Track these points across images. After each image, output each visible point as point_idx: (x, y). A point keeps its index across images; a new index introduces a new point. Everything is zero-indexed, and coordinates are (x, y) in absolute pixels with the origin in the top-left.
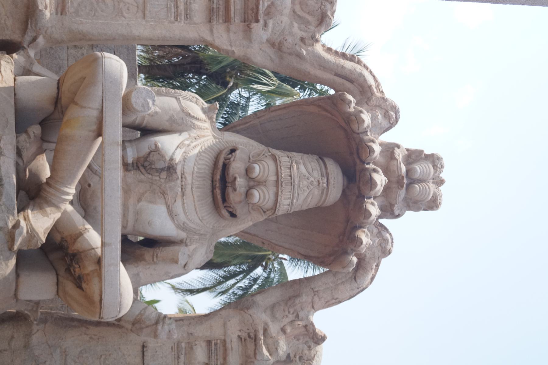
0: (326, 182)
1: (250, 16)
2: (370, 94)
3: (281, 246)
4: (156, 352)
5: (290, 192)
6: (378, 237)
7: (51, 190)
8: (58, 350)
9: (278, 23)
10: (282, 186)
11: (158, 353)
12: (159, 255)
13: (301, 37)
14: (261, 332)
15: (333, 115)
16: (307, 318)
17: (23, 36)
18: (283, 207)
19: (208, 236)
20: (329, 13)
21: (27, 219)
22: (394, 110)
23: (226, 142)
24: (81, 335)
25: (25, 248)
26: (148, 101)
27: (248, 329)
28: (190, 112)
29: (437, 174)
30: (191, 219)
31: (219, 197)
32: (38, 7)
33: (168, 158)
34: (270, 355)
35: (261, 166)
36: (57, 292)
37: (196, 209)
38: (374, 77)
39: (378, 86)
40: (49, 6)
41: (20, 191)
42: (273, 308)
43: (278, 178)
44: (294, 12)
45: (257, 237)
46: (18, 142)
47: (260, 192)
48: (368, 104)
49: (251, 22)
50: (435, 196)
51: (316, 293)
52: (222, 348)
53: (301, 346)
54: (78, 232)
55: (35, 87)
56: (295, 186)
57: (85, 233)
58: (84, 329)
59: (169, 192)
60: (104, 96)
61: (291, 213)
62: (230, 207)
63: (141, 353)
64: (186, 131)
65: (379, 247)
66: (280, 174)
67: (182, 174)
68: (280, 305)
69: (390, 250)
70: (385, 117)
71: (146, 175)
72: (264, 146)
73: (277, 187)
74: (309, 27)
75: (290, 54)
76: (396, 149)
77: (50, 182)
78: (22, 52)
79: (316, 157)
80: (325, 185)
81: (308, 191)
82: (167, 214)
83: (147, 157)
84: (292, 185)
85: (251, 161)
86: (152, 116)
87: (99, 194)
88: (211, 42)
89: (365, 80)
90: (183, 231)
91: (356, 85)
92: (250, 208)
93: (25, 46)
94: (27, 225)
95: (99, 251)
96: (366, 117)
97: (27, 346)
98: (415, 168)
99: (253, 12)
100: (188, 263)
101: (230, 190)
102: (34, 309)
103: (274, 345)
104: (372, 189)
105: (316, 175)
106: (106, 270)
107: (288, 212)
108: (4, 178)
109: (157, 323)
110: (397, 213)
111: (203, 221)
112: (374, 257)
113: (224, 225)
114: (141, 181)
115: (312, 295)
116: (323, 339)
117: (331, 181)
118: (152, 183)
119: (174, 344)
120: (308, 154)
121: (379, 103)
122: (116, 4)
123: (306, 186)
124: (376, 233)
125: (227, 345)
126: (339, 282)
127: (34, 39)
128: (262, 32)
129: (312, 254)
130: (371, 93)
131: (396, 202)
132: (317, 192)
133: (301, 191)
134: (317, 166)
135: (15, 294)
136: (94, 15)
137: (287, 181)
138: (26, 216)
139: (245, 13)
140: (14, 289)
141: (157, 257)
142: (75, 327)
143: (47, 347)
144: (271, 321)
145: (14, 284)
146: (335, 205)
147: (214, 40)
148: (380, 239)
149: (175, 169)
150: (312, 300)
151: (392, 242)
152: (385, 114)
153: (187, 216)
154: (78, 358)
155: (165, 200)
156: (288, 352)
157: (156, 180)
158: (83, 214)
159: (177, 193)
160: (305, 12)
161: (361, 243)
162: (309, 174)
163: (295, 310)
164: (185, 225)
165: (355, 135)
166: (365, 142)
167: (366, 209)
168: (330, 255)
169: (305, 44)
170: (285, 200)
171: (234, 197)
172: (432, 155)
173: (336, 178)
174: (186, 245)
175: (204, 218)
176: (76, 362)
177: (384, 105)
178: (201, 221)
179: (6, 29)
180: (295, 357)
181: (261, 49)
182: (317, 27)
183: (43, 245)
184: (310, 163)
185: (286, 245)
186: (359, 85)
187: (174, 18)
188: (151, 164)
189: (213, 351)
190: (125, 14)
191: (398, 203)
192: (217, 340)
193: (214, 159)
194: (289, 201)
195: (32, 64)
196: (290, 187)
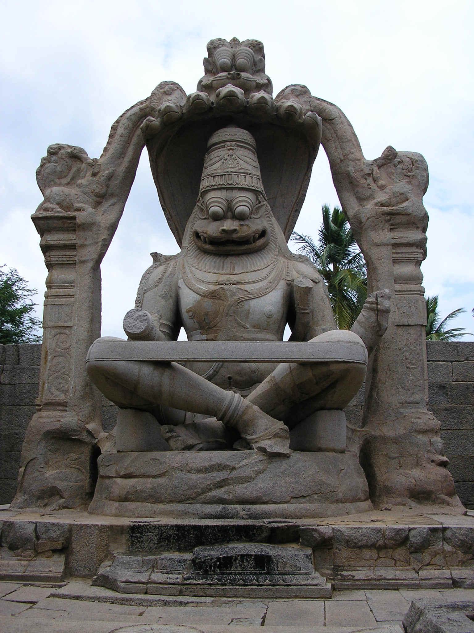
2: (148, 110)
3: (299, 193)
8: (402, 410)
9: (78, 198)
10: (232, 184)
12: (303, 307)
14: (385, 208)
17: (86, 443)
18: (254, 183)
19: (286, 261)
20: (69, 150)
21: (257, 440)
23: (190, 244)
25: (288, 442)
26: (137, 317)
28: (157, 279)
30: (266, 276)
32: (58, 429)
34: (408, 200)
36: (337, 409)
37: (255, 271)
38: (132, 107)
39: (141, 103)
40: (57, 419)
41: (234, 447)
42: (361, 200)
43: (224, 188)
44: (68, 184)
45: (290, 216)
47: (237, 205)
49: (75, 224)
53: (399, 171)
58: (380, 385)
60: (126, 359)
61: (260, 176)
62: (254, 236)
64: (177, 283)
65: (299, 97)
66: (220, 186)
68: (357, 192)
69: (303, 87)
75: (108, 186)
77: (220, 416)
78: (101, 446)
80: (233, 143)
81: (238, 160)
88: (94, 262)
89: (134, 114)
91: (140, 122)
93: (96, 441)
94: (263, 440)
95: (293, 365)
97: (396, 441)
98: (220, 64)
101: (235, 236)
102: (358, 434)
103: (398, 196)
104: (236, 95)
107: (259, 179)
108: (212, 463)
111: (269, 264)
112: (310, 102)
115: (348, 160)
117: (229, 138)
119: (396, 295)
121: (156, 100)
122: (57, 353)
127: (89, 432)
128: (84, 213)
131: (254, 81)
132: (241, 152)
134: (214, 152)
137: (227, 179)
138: (253, 441)
139: (68, 231)
142: (378, 393)
143: (397, 421)
144: (374, 198)
145: (327, 453)
147: (93, 259)
149: (213, 292)
150: (353, 161)
152: (167, 94)
154: (409, 390)
159: (238, 288)
160: (68, 173)
161: (292, 106)
166: (190, 106)
167: (257, 103)
169: (98, 172)
170: (247, 181)
172: (209, 49)
173: (227, 133)
175: (266, 263)
176: (412, 394)
179: (80, 460)
181: (103, 215)
182: (82, 161)
183: (285, 424)
186: (139, 120)
187: (72, 298)
189: (404, 256)
192: (393, 253)
194: (247, 177)
196: (233, 175)
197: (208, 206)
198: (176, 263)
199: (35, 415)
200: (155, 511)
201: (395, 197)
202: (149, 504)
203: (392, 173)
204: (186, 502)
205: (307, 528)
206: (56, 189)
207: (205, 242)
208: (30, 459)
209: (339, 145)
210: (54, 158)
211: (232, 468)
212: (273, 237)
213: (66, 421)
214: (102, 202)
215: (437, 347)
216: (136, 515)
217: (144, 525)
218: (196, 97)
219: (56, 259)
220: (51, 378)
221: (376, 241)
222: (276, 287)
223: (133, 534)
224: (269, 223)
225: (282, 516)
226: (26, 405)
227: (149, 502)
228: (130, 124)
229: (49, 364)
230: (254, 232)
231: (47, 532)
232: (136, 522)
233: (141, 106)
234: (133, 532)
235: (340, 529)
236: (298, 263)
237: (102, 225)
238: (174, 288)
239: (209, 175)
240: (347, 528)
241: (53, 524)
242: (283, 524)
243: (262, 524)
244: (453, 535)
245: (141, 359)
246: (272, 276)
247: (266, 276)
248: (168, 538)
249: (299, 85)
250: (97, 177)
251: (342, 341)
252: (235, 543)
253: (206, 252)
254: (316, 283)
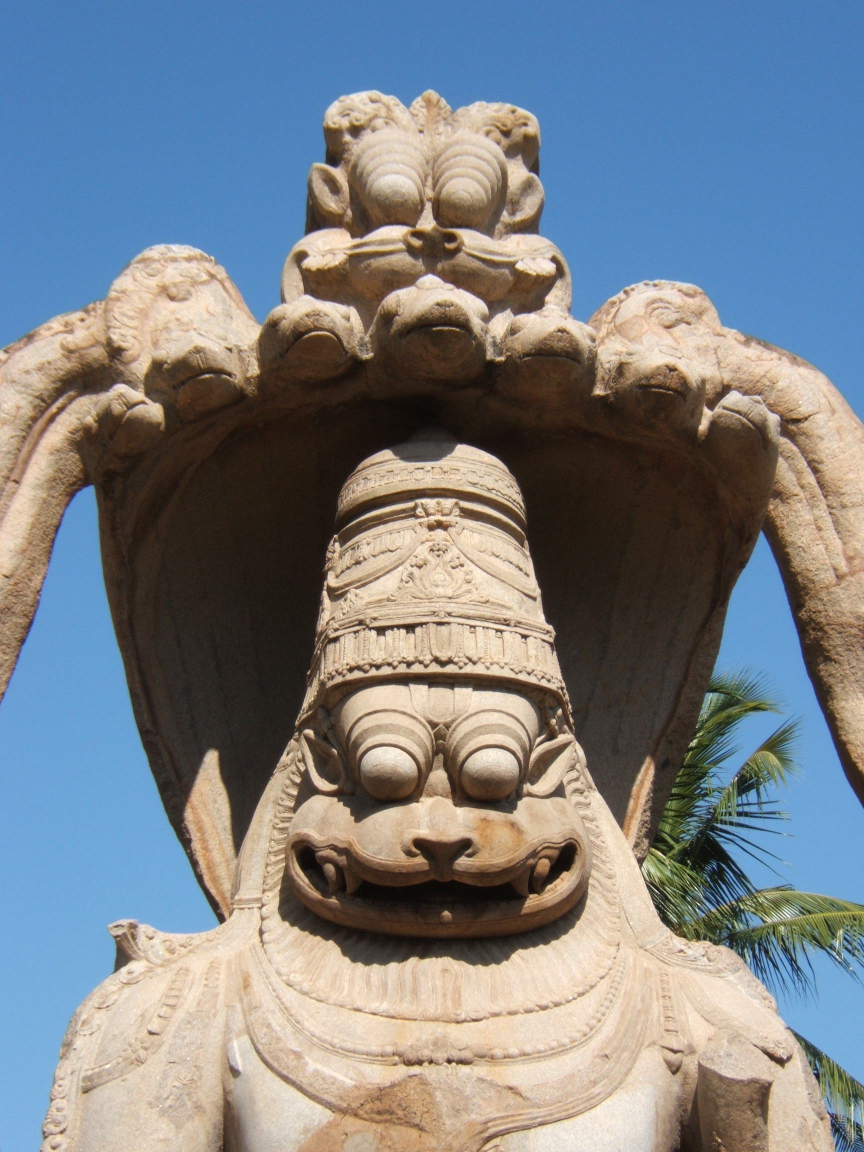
0: (436, 500)
2: (98, 353)
3: (678, 695)
10: (450, 661)
18: (533, 660)
22: (156, 266)
30: (586, 1029)
37: (544, 1008)
48: (134, 360)
50: (485, 125)
56: (449, 610)
59: (473, 1116)
61: (554, 633)
65: (675, 330)
66: (402, 669)
70: (184, 299)
72: (292, 742)
76: (308, 263)
79: (335, 547)
80: (448, 503)
81: (469, 566)
84: (449, 623)
89: (40, 369)
90: (634, 1059)
100: (761, 1044)
111: (592, 979)
113: (602, 901)
123: (450, 575)
124: (626, 342)
130: (93, 346)
133: (469, 591)
148: (646, 327)
149: (381, 1093)
152: (172, 298)
153: (574, 1045)
155: (507, 1132)
159: (482, 1080)
162: (403, 563)
164: (607, 1052)
170: (507, 651)
177: (140, 298)
178: (592, 987)
184: (358, 563)
186: (59, 392)
191: (512, 259)
197: (357, 745)
207: (340, 888)
209: (829, 519)
212: (599, 870)
218: (309, 322)
222: (626, 1074)
224: (582, 812)
228: (23, 403)
230: (534, 854)
233: (70, 338)
236: (699, 977)
239: (361, 623)
246: (608, 1028)
247: (586, 1029)
254: (781, 1062)
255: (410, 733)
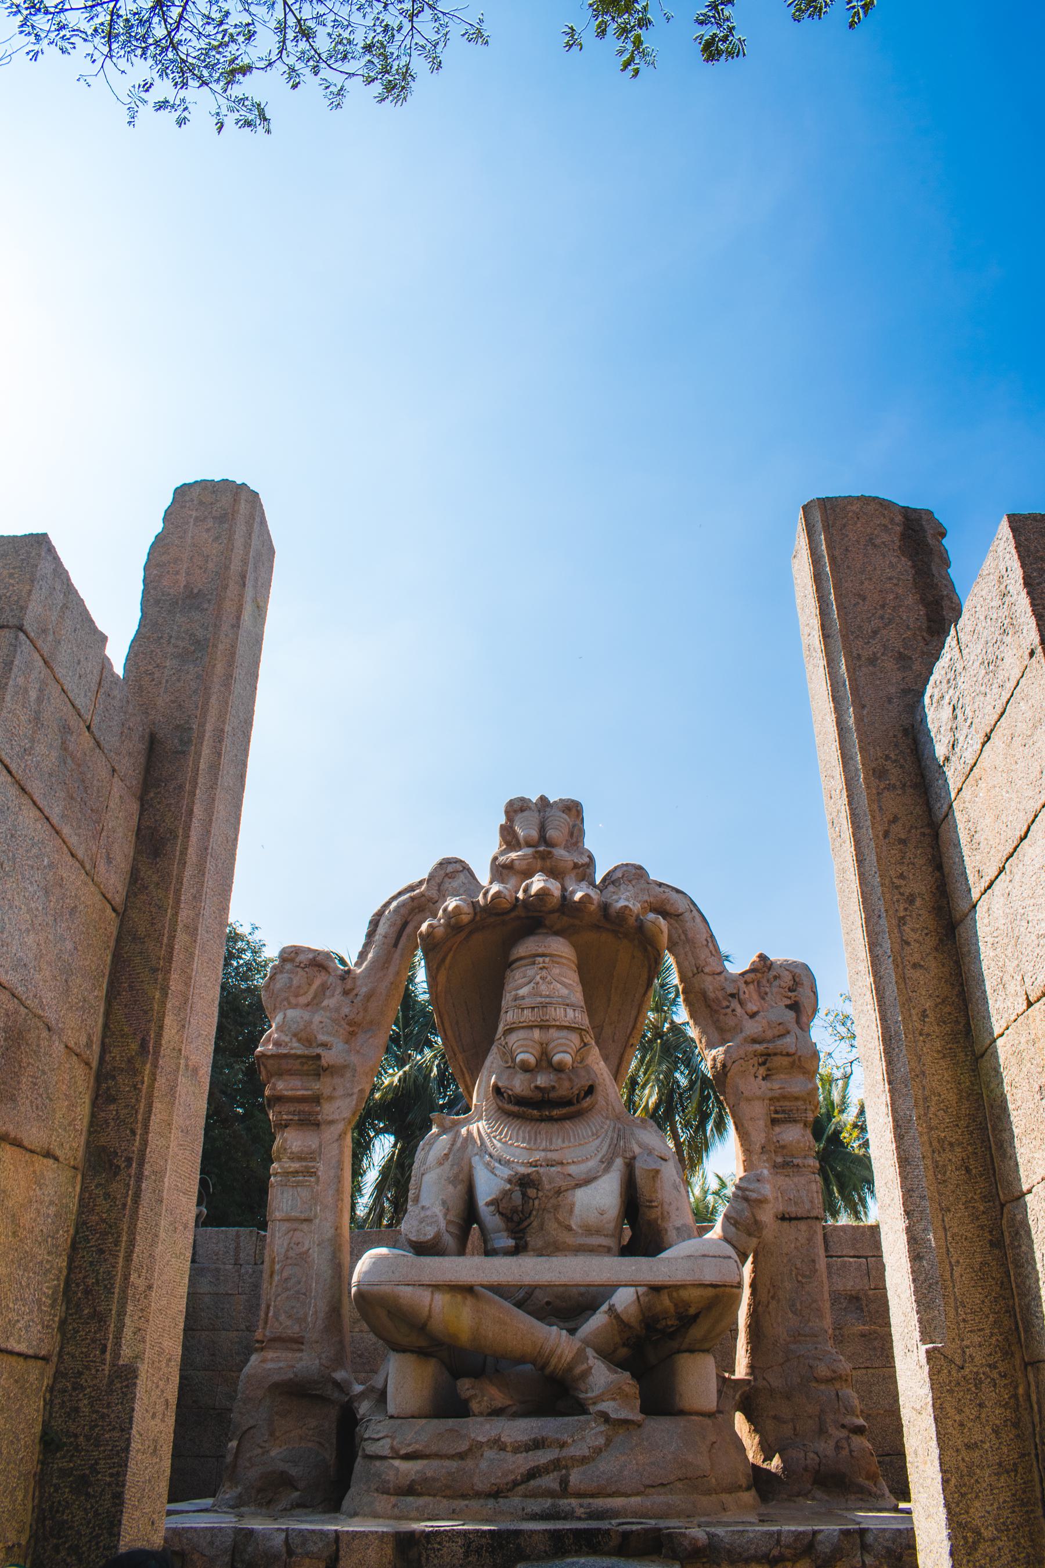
1: (311, 1068)
4: (790, 1199)
5: (555, 1009)
6: (620, 885)
7: (554, 1361)
8: (792, 1347)
10: (547, 1020)
11: (792, 1197)
13: (343, 995)
14: (757, 1047)
15: (451, 950)
16: (733, 979)
20: (311, 956)
21: (594, 1400)
22: (445, 866)
24: (769, 1313)
27: (753, 1066)
29: (533, 807)
31: (564, 1111)
32: (291, 1380)
33: (508, 1186)
34: (788, 1032)
35: (518, 1051)
36: (703, 1351)
37: (581, 1144)
38: (400, 894)
39: (411, 888)
43: (536, 1026)
46: (481, 1414)
49: (319, 1066)
51: (699, 970)
52: (781, 1103)
54: (614, 1321)
55: (402, 1387)
57: (616, 1310)
62: (578, 1094)
63: (794, 1222)
64: (470, 1159)
65: (634, 882)
66: (531, 1024)
67: (531, 1165)
71: (532, 1218)
72: (493, 1047)
73: (548, 1027)
74: (329, 983)
78: (356, 1404)
79: (508, 972)
80: (547, 959)
81: (555, 983)
82: (589, 1186)
83: (506, 1217)
85: (512, 1065)
86: (448, 1209)
87: (561, 1289)
92: (579, 1065)
93: (346, 1399)
94: (603, 1401)
95: (641, 1290)
96: (452, 903)
99: (306, 1063)
101: (553, 1095)
105: (531, 972)
106: (668, 1279)
108: (533, 1436)
109: (746, 1199)
110: (586, 860)
114: (541, 1227)
116: (762, 957)
117: (540, 951)
118: (544, 1210)
120: (504, 984)
122: (289, 1261)
125: (777, 1095)
126: (683, 937)
127: (337, 1384)
128: (334, 1050)
129: (645, 976)
132: (556, 971)
135: (709, 1416)
136: (305, 1294)
138: (590, 1401)
139: (308, 1075)
140: (701, 1418)
141: (651, 1201)
144: (741, 1032)
145: (693, 1418)
146: (575, 946)
147: (344, 1119)
150: (709, 975)
151: (627, 865)
155: (568, 1190)
156: (784, 1007)
157: (539, 1204)
158: (590, 1312)
159: (559, 1172)
160: (308, 990)
161: (626, 907)
163: (725, 998)
165: (478, 918)
168: (646, 950)
171: (564, 1090)
172: (507, 812)
174: (634, 1158)
180: (790, 998)
181: (358, 1052)
183: (633, 1376)
185: (634, 1013)
188: (514, 1210)
190: (305, 1249)
193: (510, 1119)
194: (568, 1010)
195: (372, 1389)
197: (515, 1052)
198: (468, 1130)
199: (254, 1358)
200: (454, 1511)
201: (770, 1027)
202: (445, 1501)
203: (766, 994)
204: (503, 1495)
205: (673, 1532)
206: (291, 1013)
208: (247, 1427)
210: (288, 966)
211: (564, 1443)
212: (602, 1091)
213: (303, 1367)
214: (357, 1033)
215: (842, 1234)
216: (426, 1516)
217: (445, 1530)
219: (291, 1117)
220: (279, 1298)
221: (746, 1094)
223: (428, 1544)
225: (635, 1515)
226: (203, 1330)
227: (444, 1497)
229: (276, 1278)
231: (303, 1544)
232: (432, 1526)
233: (412, 894)
234: (428, 1543)
235: (717, 1532)
236: (637, 1131)
237: (358, 1069)
238: (466, 1168)
240: (727, 1532)
241: (313, 1531)
242: (639, 1527)
243: (609, 1527)
244: (876, 1540)
245: (434, 1283)
248: (478, 1551)
249: (632, 865)
250: (351, 996)
251: (708, 1256)
252: (573, 1556)
253: (509, 1114)
254: (666, 1160)
255: (533, 1047)
